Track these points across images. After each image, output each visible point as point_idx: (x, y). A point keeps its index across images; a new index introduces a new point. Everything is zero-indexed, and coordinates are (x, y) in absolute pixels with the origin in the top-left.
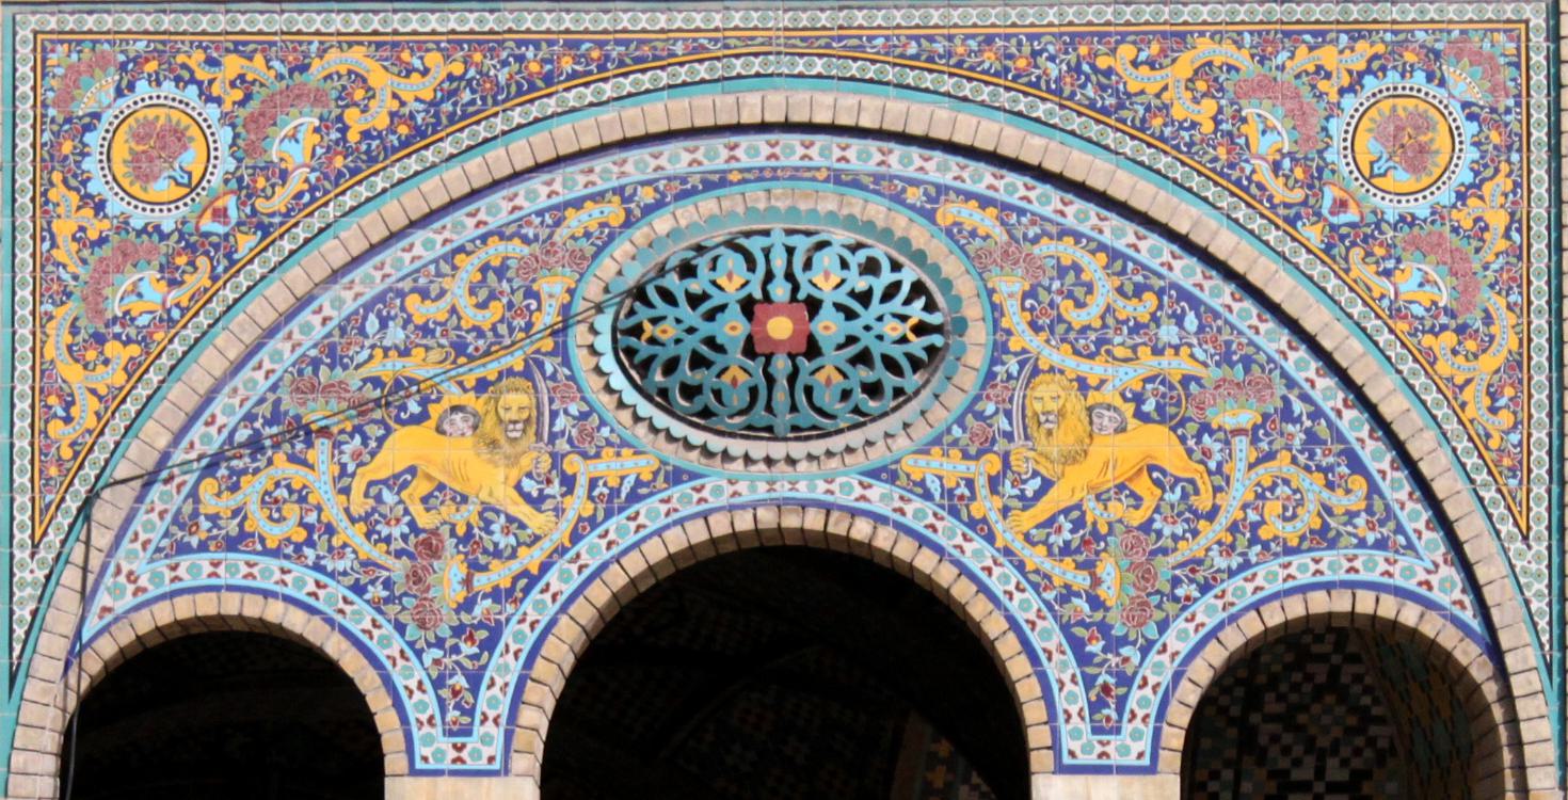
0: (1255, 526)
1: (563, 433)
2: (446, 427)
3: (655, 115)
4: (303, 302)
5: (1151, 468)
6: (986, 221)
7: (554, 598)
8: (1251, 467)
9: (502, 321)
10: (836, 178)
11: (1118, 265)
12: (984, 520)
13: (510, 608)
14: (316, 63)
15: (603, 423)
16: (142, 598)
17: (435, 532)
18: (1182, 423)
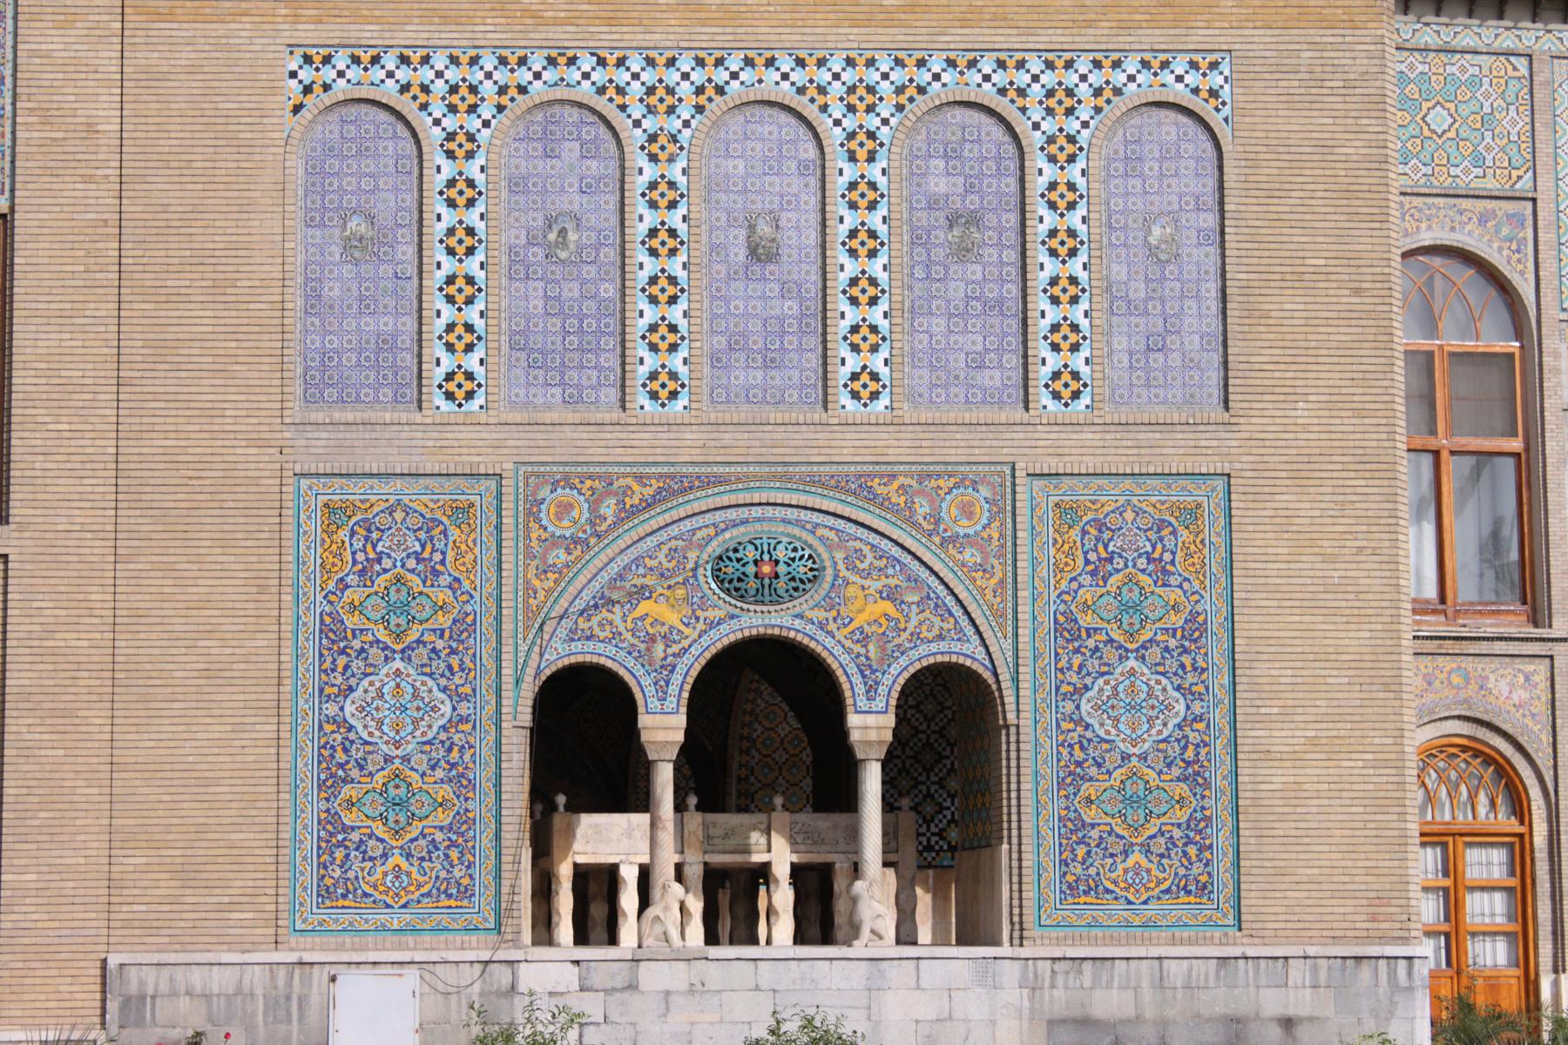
3: (726, 500)
4: (611, 560)
6: (831, 535)
10: (783, 520)
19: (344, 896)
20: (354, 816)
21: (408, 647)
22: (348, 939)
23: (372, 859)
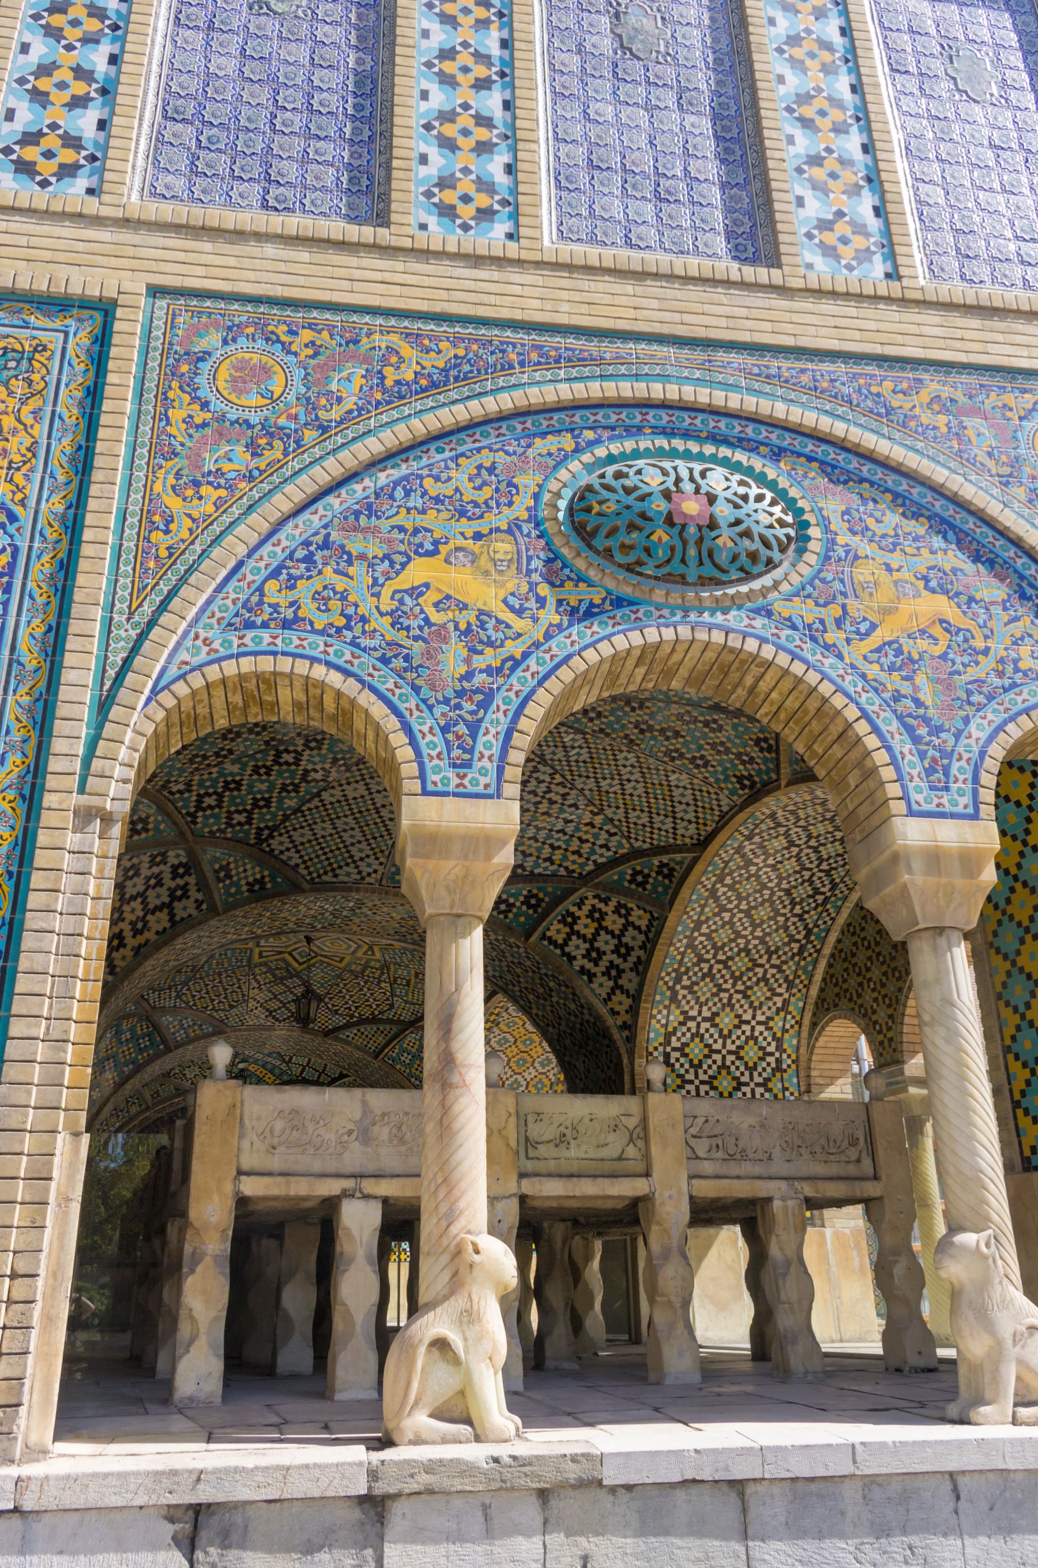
0: (1015, 662)
1: (536, 570)
2: (453, 560)
5: (942, 621)
7: (533, 675)
8: (1006, 624)
9: (491, 498)
11: (900, 501)
12: (834, 645)
13: (501, 680)
14: (364, 340)
15: (565, 566)
16: (213, 656)
17: (444, 626)
18: (958, 594)
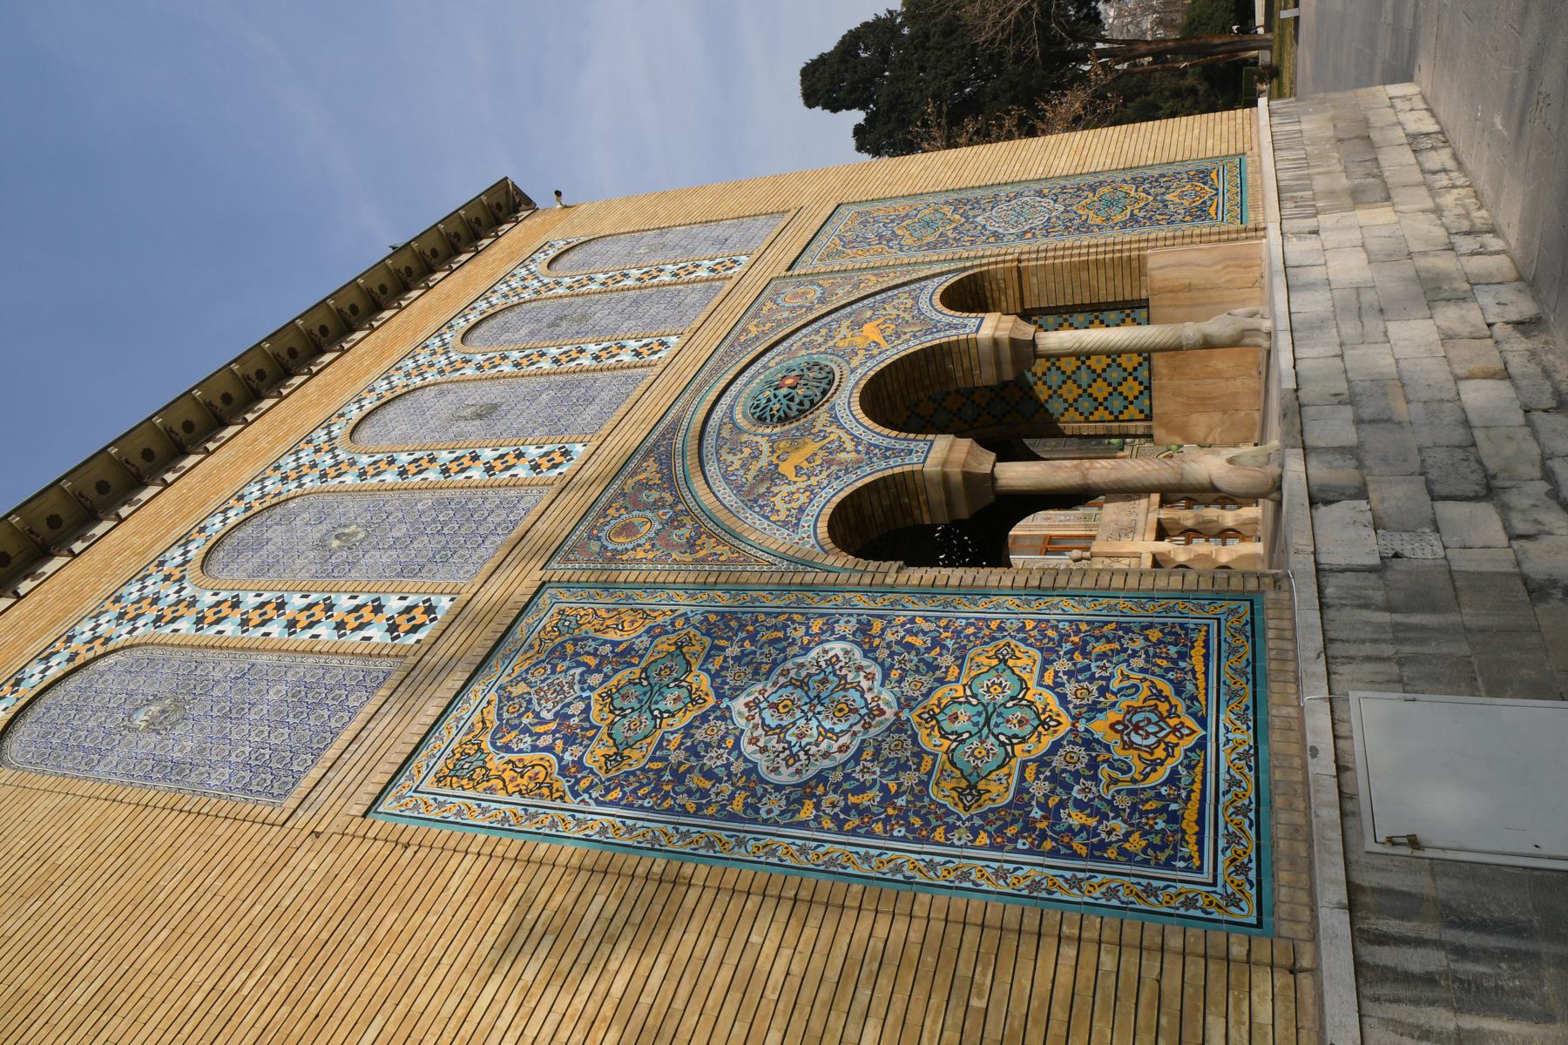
19: (1174, 818)
20: (995, 788)
21: (716, 690)
22: (1282, 821)
23: (1093, 765)
